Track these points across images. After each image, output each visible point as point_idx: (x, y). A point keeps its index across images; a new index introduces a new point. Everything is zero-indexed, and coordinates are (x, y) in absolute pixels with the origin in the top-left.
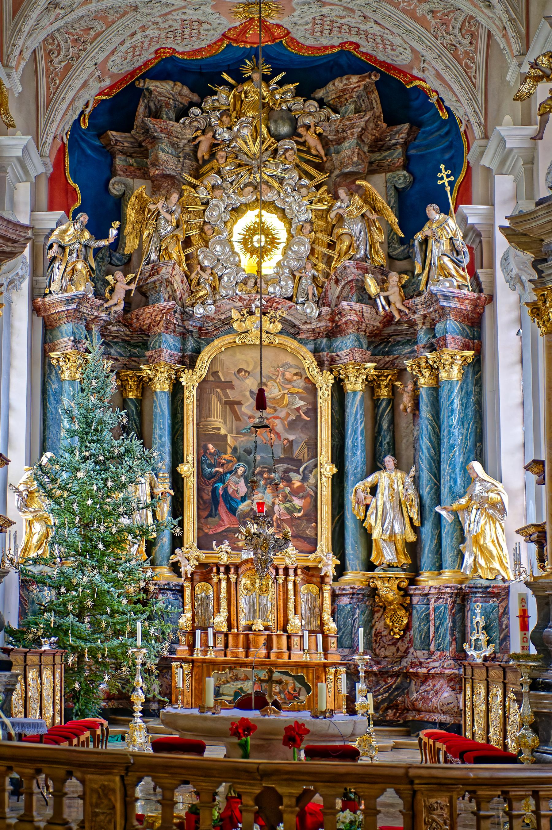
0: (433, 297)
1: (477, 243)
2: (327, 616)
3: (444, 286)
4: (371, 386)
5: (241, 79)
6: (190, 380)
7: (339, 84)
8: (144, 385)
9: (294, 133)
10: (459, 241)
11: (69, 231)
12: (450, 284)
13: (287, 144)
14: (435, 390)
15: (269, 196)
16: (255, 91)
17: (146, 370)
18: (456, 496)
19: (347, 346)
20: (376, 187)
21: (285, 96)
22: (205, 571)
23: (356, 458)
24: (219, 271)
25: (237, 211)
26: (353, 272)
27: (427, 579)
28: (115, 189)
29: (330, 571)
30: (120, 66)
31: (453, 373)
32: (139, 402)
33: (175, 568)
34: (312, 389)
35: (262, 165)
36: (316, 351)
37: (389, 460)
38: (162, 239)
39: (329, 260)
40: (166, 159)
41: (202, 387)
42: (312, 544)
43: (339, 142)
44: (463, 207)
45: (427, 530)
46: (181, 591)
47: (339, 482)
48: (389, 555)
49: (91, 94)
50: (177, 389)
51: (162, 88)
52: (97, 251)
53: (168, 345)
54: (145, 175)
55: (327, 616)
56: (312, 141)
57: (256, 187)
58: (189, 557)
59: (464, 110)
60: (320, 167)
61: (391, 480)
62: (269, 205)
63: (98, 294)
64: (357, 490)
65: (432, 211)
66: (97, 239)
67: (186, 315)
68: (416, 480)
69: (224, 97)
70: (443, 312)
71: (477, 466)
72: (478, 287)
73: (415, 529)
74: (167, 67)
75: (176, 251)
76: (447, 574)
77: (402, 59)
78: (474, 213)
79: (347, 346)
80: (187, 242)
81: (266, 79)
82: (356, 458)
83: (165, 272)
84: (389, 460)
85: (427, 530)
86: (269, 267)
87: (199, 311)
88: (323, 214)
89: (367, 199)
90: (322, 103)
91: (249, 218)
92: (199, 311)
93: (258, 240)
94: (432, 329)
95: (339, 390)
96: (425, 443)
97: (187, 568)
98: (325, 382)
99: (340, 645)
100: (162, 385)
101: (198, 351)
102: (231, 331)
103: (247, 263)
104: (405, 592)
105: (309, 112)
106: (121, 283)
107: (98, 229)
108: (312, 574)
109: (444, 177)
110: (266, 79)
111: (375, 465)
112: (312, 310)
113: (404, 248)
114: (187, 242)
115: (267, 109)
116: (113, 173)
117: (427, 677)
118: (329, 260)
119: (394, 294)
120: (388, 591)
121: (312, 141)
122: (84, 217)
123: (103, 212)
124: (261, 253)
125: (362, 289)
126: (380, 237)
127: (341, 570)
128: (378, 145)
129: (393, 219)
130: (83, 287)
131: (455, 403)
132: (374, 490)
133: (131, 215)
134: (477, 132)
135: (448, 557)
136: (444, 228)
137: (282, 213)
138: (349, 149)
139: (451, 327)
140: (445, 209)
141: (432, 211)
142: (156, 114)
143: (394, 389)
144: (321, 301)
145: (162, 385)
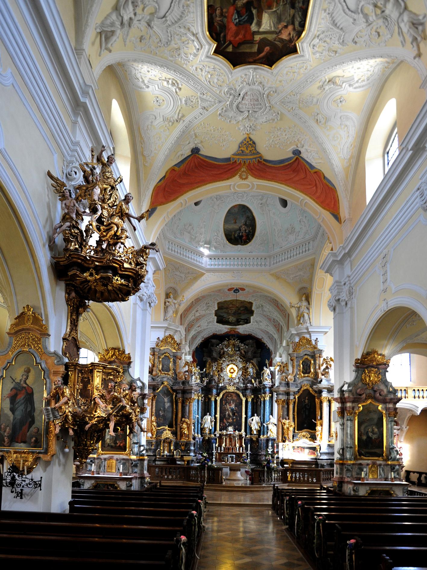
0: (264, 385)
1: (272, 374)
2: (243, 444)
3: (266, 383)
4: (253, 399)
5: (229, 339)
6: (218, 399)
7: (248, 341)
8: (210, 399)
9: (239, 350)
10: (269, 374)
11: (196, 370)
12: (267, 382)
13: (238, 352)
14: (264, 401)
15: (234, 362)
16: (232, 342)
17: (210, 396)
18: (267, 422)
19: (248, 392)
20: (254, 361)
21: (237, 342)
22: (221, 435)
23: (250, 414)
24: (225, 377)
25: (228, 365)
26: (250, 379)
27: (261, 436)
28: (204, 360)
29: (244, 436)
30: (206, 334)
31: (267, 399)
32: (208, 402)
33: (215, 435)
34: (242, 400)
35: (233, 357)
36: (242, 393)
37: (256, 415)
38: (213, 371)
39: (245, 376)
40: (215, 355)
41: (221, 400)
42: (240, 430)
43: (248, 352)
44: (270, 367)
45: (262, 428)
46: (216, 439)
47: (246, 419)
48: (255, 432)
49: (200, 341)
50: (216, 401)
51: (214, 341)
52: (201, 374)
53: (214, 391)
54: (210, 357)
55: (243, 444)
56: (243, 352)
57: (232, 361)
58: (218, 433)
59: (271, 348)
60: (244, 357)
61: (256, 418)
62: (234, 364)
63: (201, 382)
64: (250, 420)
65: (265, 369)
66: (201, 371)
67: (218, 386)
68: (260, 418)
69: (226, 342)
70: (266, 387)
71: (271, 416)
72: (272, 382)
73: (260, 428)
74: (215, 336)
75: (216, 373)
76: (265, 436)
77: (260, 337)
78: (272, 368)
79: (248, 392)
80: (218, 371)
81: (234, 340)
82: (250, 414)
83: (214, 378)
84: (256, 415)
85: (262, 428)
86: (234, 375)
87: (220, 385)
88: (244, 367)
89: (253, 364)
90: (245, 344)
91: (231, 366)
92: (220, 385)
93: (232, 371)
94: (264, 390)
95: (247, 402)
96: (262, 411)
97: (218, 435)
98: (244, 400)
99: (245, 449)
100: (213, 399)
101: (220, 393)
102: (226, 389)
103: (230, 375)
104: (257, 439)
105: (242, 346)
106: (206, 380)
107: (201, 369)
108: (240, 437)
109: (267, 362)
110: (234, 340)
111: (253, 415)
112: (242, 385)
113: (259, 375)
114: (218, 371)
115: (234, 345)
116: (204, 356)
117: (261, 455)
118: (245, 376)
119: (257, 382)
120: (254, 439)
121: (243, 352)
122: (199, 367)
123: (201, 364)
124: (233, 373)
125: (251, 381)
126: (255, 372)
127: (246, 435)
128: (255, 353)
129: (257, 368)
130: (198, 381)
131: (267, 404)
132: (252, 420)
133: (208, 366)
134: (273, 352)
135: (265, 433)
136: (267, 371)
137: (237, 366)
138: (250, 354)
139: (267, 390)
140: (267, 368)
141: (265, 369)
142: (213, 346)
143: (257, 400)
144: (244, 384)
145: (213, 399)
